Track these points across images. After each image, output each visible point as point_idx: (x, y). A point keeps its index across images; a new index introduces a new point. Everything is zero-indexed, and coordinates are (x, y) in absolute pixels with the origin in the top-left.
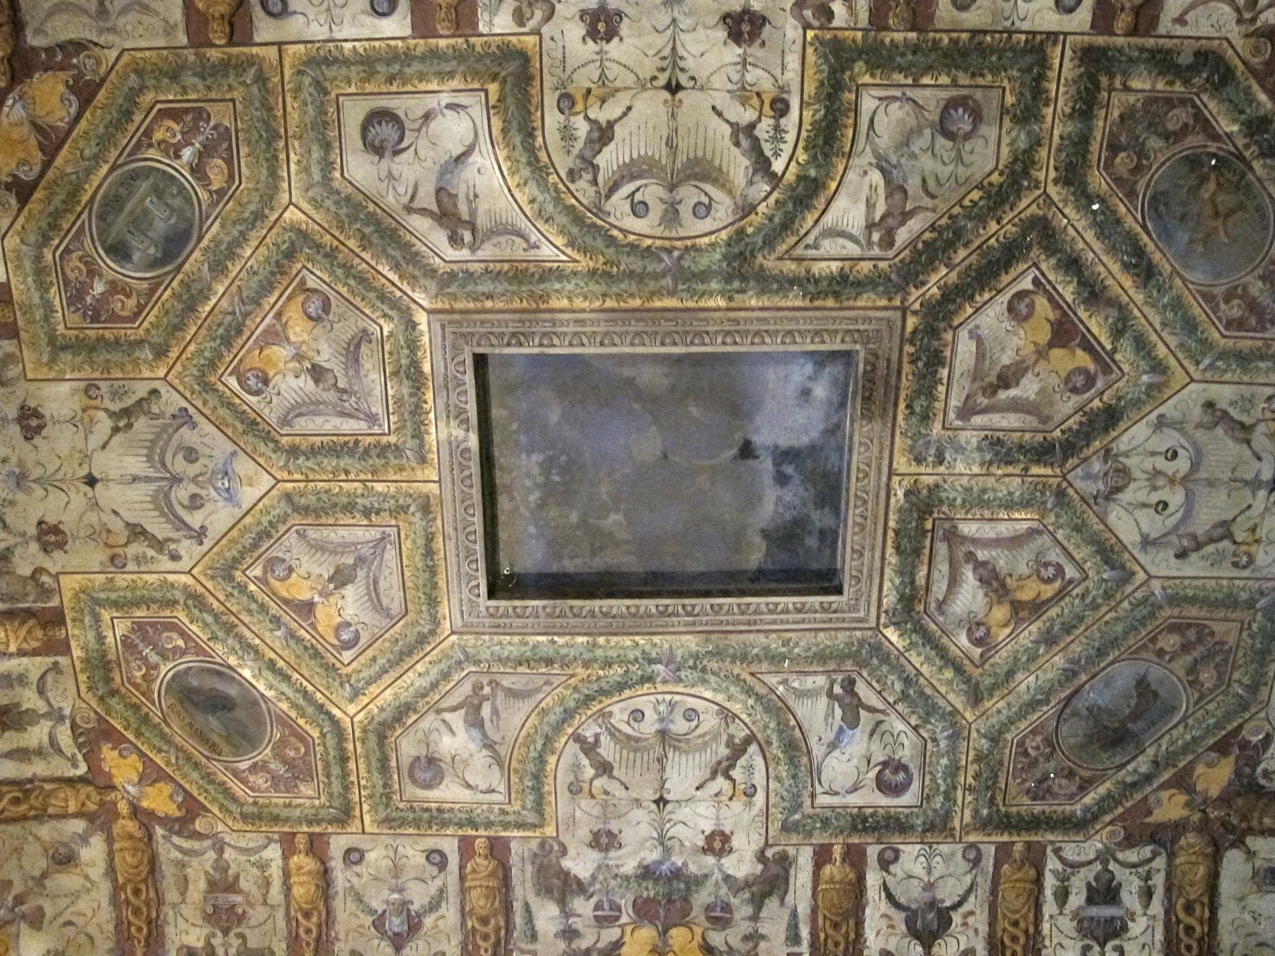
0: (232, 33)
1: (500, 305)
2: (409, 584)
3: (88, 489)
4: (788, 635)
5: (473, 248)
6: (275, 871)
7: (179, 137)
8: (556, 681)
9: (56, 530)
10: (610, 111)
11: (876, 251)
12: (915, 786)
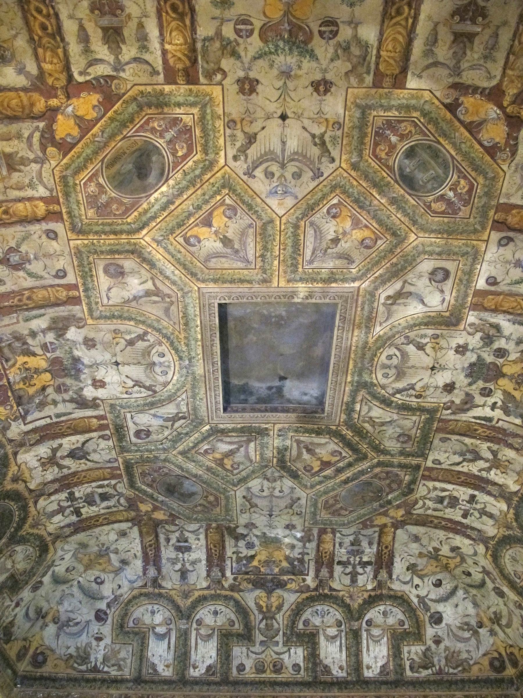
0: (498, 222)
1: (358, 313)
2: (224, 271)
3: (279, 114)
4: (205, 400)
5: (384, 304)
6: (29, 193)
7: (459, 191)
8: (177, 327)
9: (252, 90)
10: (428, 349)
11: (361, 418)
12: (140, 441)
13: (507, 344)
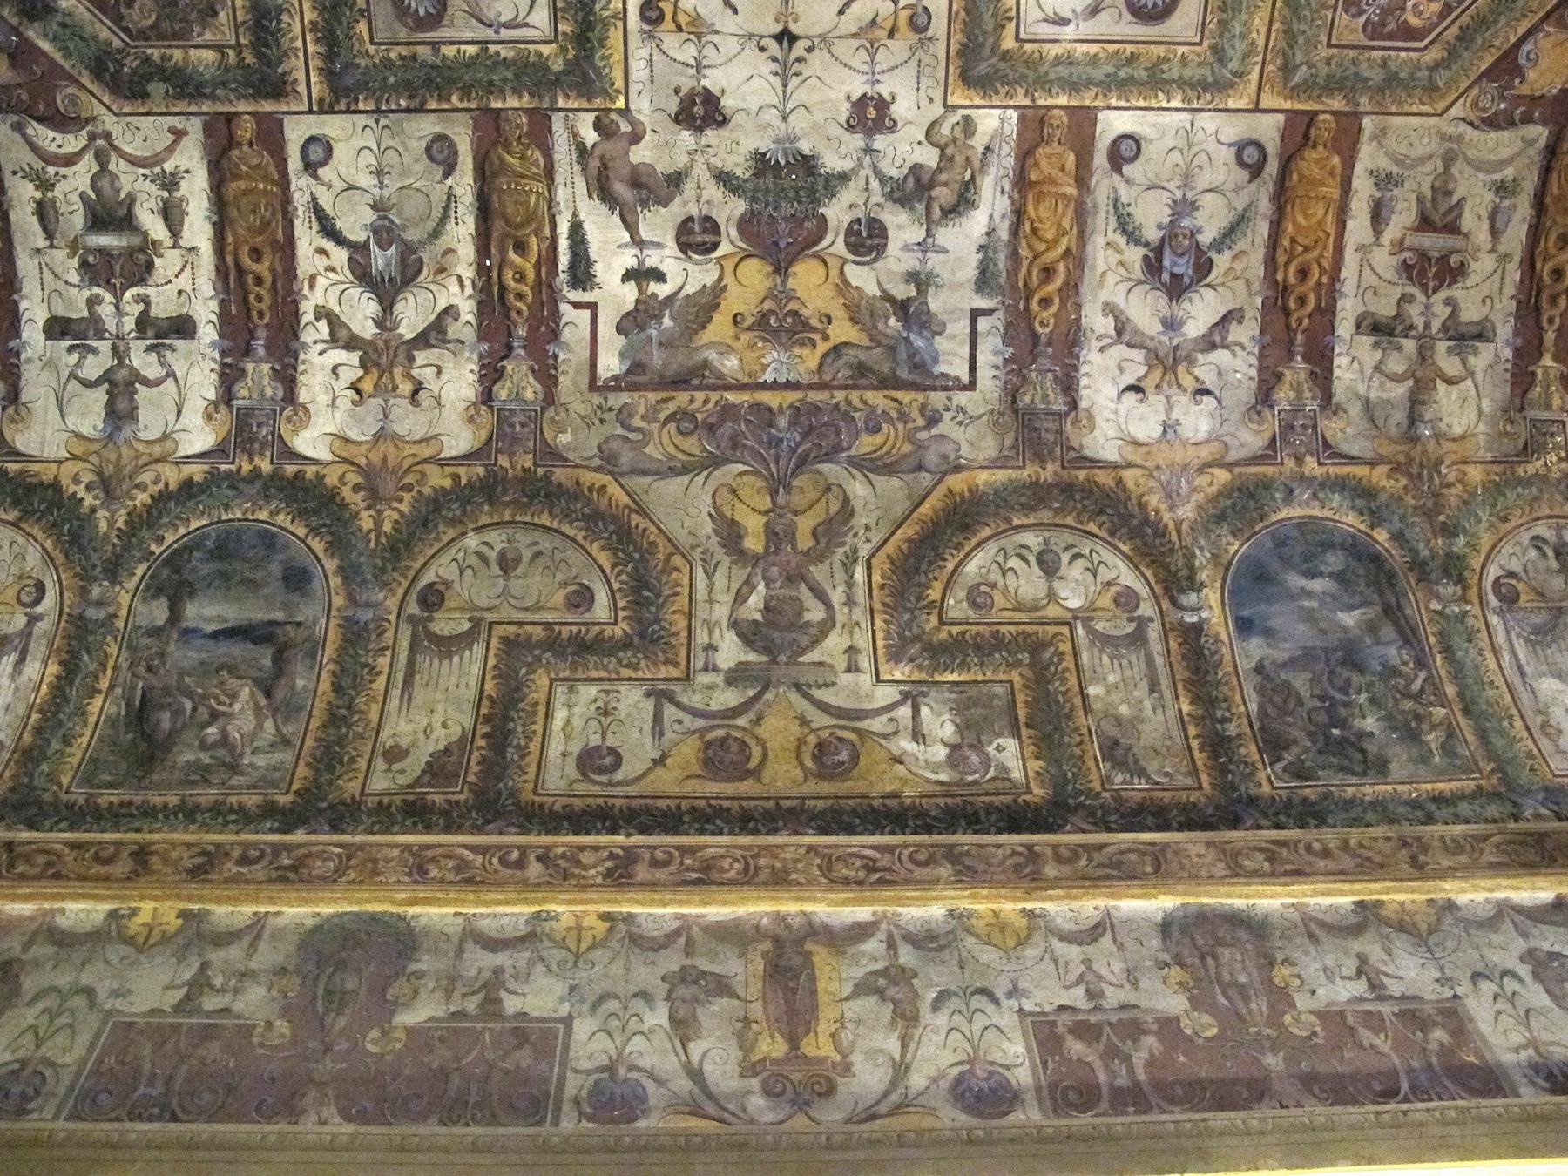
0: (1309, 126)
13: (906, 248)
